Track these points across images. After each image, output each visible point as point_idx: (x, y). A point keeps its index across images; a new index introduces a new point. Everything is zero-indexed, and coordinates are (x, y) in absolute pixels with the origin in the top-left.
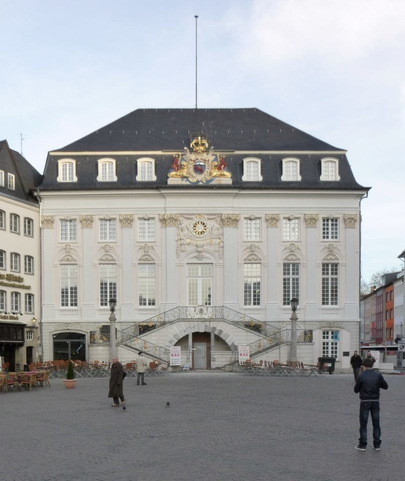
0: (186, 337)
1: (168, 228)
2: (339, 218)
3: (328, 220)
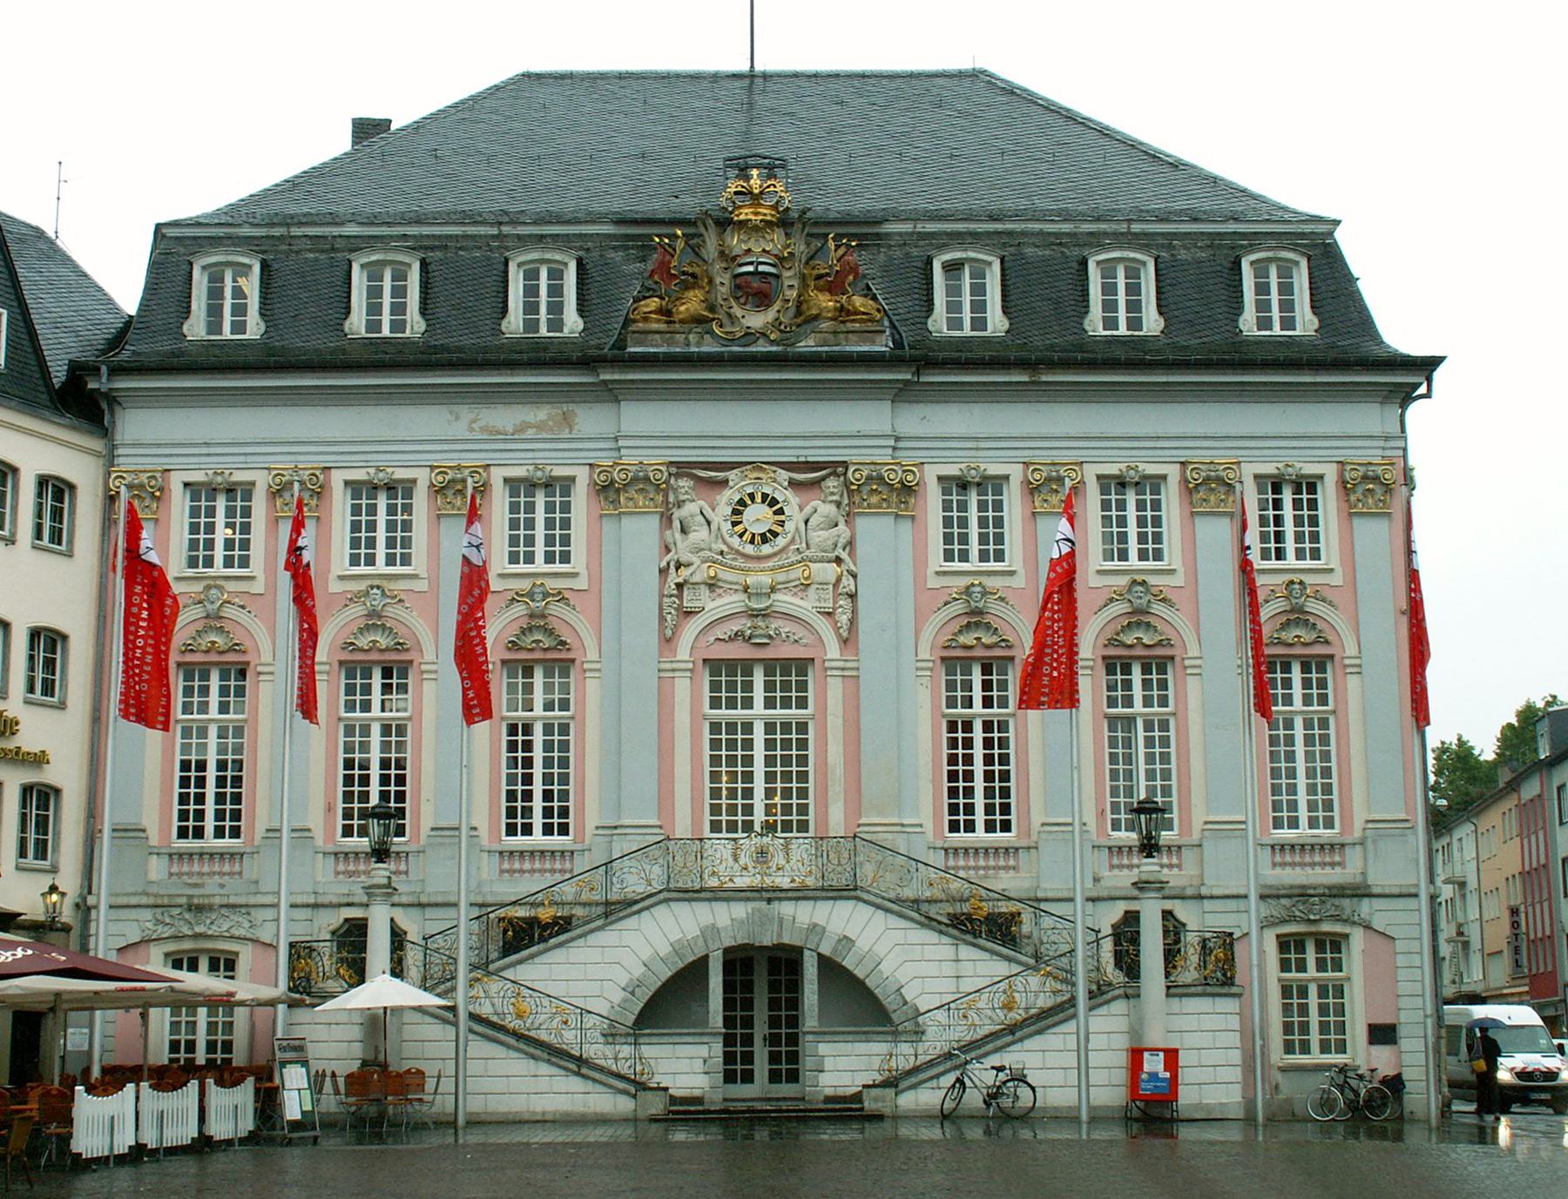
0: (702, 964)
1: (625, 521)
2: (1321, 477)
3: (1277, 489)
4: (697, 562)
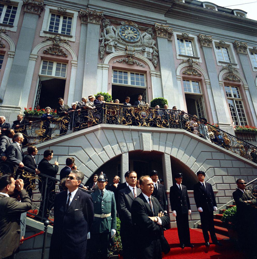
1: (89, 25)
4: (111, 40)
